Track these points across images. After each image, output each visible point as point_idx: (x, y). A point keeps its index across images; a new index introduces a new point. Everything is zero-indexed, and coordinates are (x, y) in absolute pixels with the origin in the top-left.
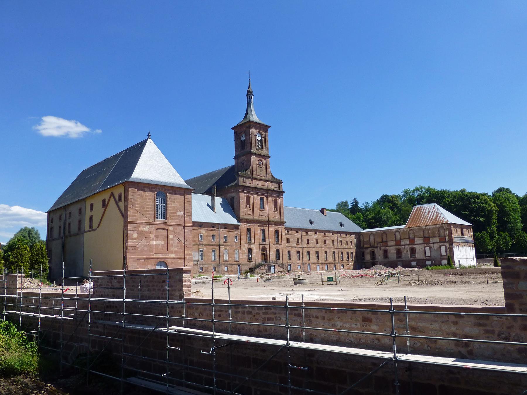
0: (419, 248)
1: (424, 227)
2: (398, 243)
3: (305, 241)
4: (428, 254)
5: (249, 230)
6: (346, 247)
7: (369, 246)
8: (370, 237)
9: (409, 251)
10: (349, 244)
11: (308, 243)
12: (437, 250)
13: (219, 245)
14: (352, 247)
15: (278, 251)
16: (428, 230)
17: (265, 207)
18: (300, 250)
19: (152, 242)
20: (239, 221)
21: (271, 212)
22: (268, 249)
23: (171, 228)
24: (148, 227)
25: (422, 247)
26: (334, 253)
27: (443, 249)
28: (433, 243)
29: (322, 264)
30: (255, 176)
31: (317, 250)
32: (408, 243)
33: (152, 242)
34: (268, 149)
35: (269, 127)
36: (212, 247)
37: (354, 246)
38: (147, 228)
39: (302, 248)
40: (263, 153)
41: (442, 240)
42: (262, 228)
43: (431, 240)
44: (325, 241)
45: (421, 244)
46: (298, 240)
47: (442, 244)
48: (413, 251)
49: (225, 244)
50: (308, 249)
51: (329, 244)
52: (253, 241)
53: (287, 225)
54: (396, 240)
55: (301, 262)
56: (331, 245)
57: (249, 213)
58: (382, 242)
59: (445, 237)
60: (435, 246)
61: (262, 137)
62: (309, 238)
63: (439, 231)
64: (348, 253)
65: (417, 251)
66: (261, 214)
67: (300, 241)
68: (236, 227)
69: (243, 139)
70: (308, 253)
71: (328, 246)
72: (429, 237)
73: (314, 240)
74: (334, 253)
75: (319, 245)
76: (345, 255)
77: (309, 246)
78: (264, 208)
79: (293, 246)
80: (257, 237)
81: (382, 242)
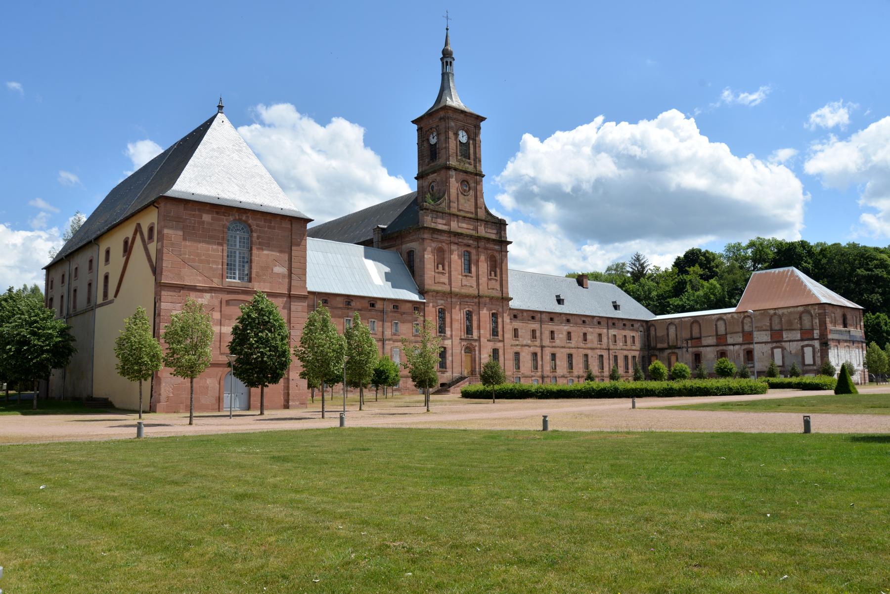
0: (760, 350)
1: (772, 312)
2: (721, 340)
3: (547, 334)
4: (778, 361)
6: (625, 347)
7: (665, 345)
8: (667, 329)
9: (742, 355)
10: (629, 341)
11: (553, 338)
12: (796, 355)
14: (634, 348)
16: (780, 317)
17: (473, 269)
18: (538, 350)
20: (422, 292)
21: (483, 280)
22: (477, 348)
24: (207, 296)
25: (767, 348)
26: (601, 356)
27: (808, 351)
28: (790, 341)
29: (579, 377)
30: (454, 210)
31: (569, 351)
32: (740, 340)
34: (480, 161)
35: (483, 119)
37: (638, 345)
38: (205, 299)
39: (542, 347)
40: (471, 168)
41: (806, 335)
43: (786, 336)
44: (585, 334)
45: (766, 343)
46: (534, 331)
47: (806, 343)
48: (749, 354)
49: (395, 337)
51: (592, 342)
53: (512, 304)
54: (717, 335)
55: (539, 374)
56: (595, 344)
57: (442, 280)
58: (692, 338)
59: (813, 329)
60: (793, 347)
61: (469, 138)
63: (800, 318)
64: (626, 357)
65: (756, 355)
66: (464, 283)
67: (538, 334)
68: (417, 307)
69: (433, 141)
70: (554, 356)
71: (589, 345)
72: (781, 330)
73: (565, 333)
74: (601, 356)
75: (573, 343)
76: (621, 362)
77: (554, 344)
78: (470, 272)
79: (525, 343)
80: (456, 325)
81: (692, 338)
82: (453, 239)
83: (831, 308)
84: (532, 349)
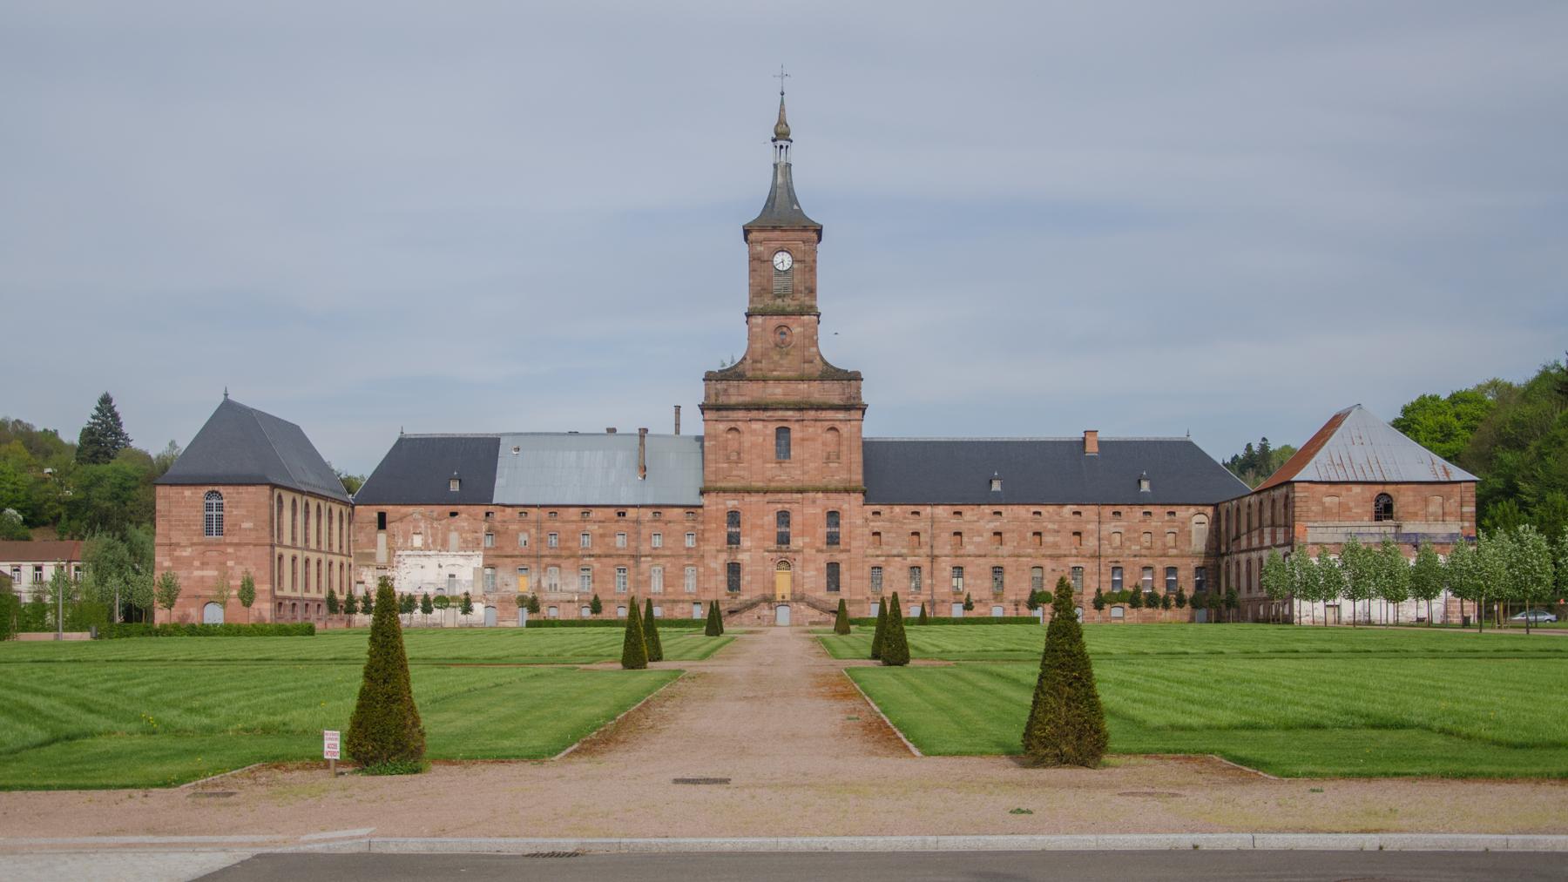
3: (946, 536)
5: (734, 517)
13: (636, 557)
15: (833, 570)
19: (197, 573)
23: (230, 550)
33: (197, 573)
36: (615, 561)
38: (187, 552)
39: (933, 558)
42: (779, 507)
50: (958, 562)
51: (1056, 545)
52: (746, 542)
62: (963, 528)
67: (923, 538)
70: (959, 571)
73: (988, 535)
75: (1006, 549)
79: (895, 552)
82: (754, 414)
83: (1324, 488)
84: (910, 561)
